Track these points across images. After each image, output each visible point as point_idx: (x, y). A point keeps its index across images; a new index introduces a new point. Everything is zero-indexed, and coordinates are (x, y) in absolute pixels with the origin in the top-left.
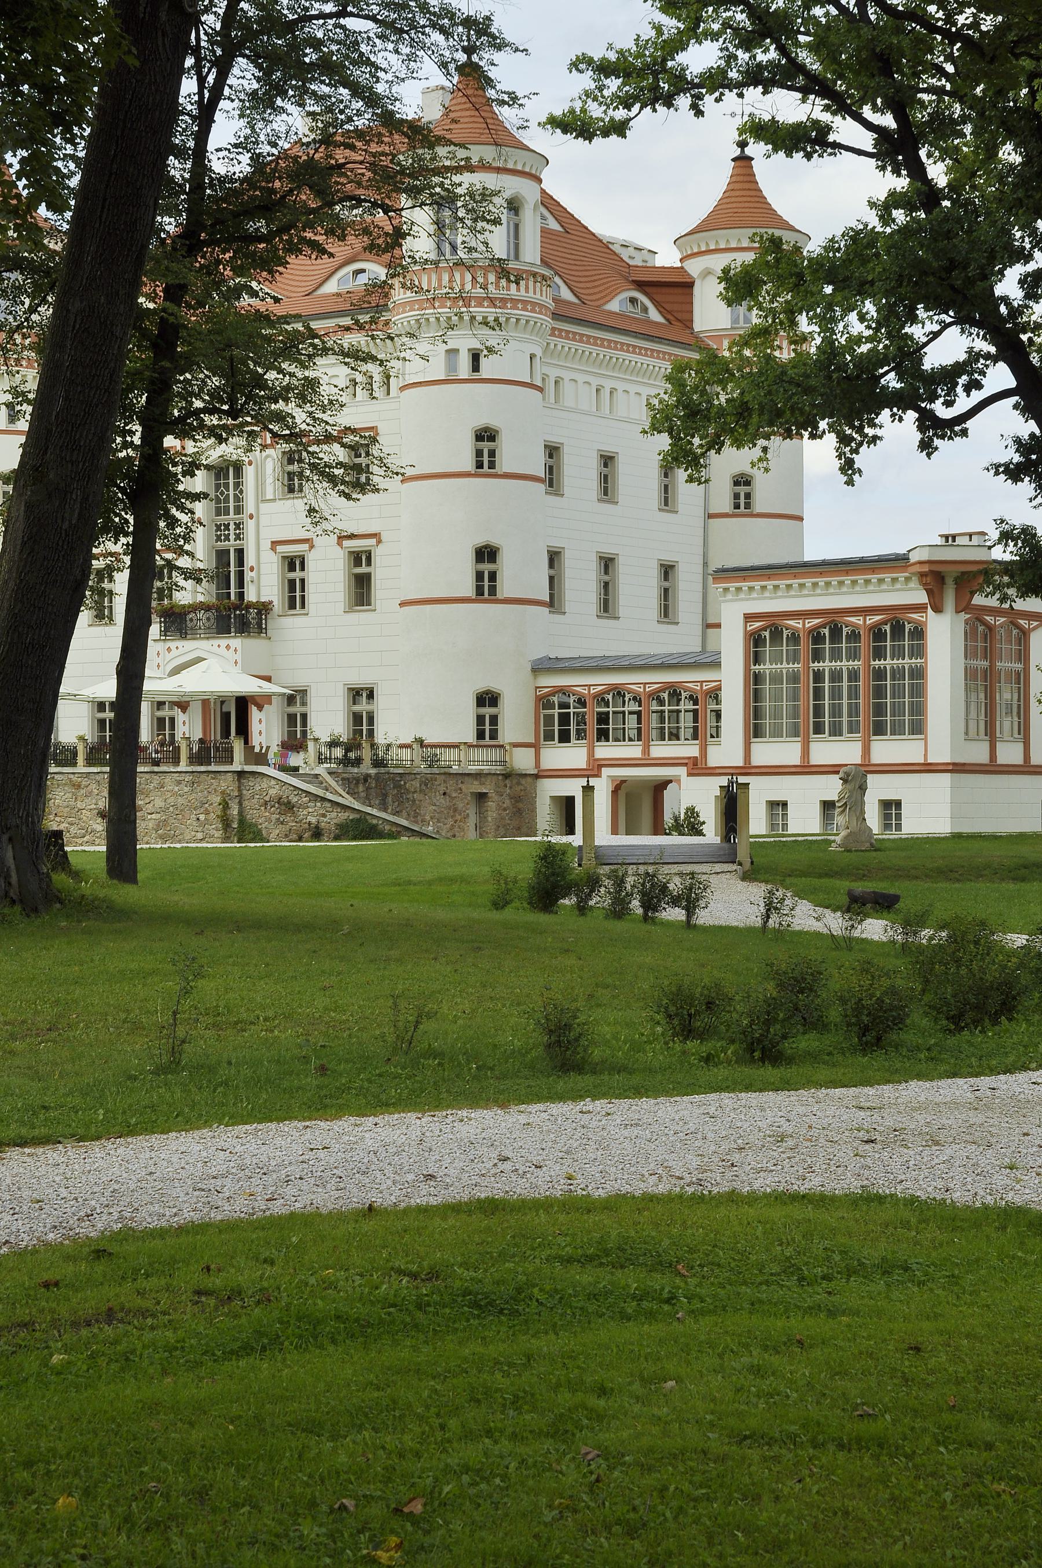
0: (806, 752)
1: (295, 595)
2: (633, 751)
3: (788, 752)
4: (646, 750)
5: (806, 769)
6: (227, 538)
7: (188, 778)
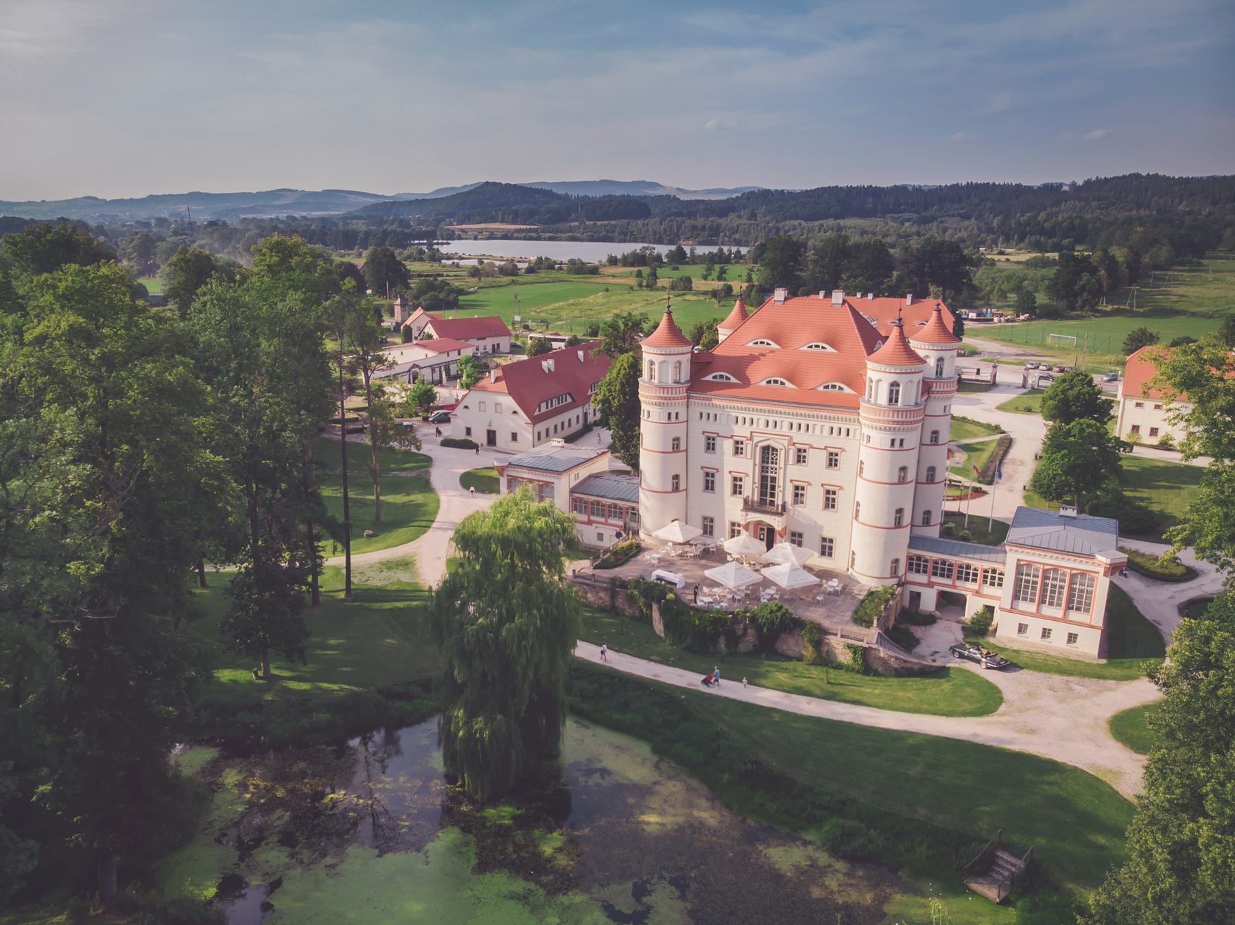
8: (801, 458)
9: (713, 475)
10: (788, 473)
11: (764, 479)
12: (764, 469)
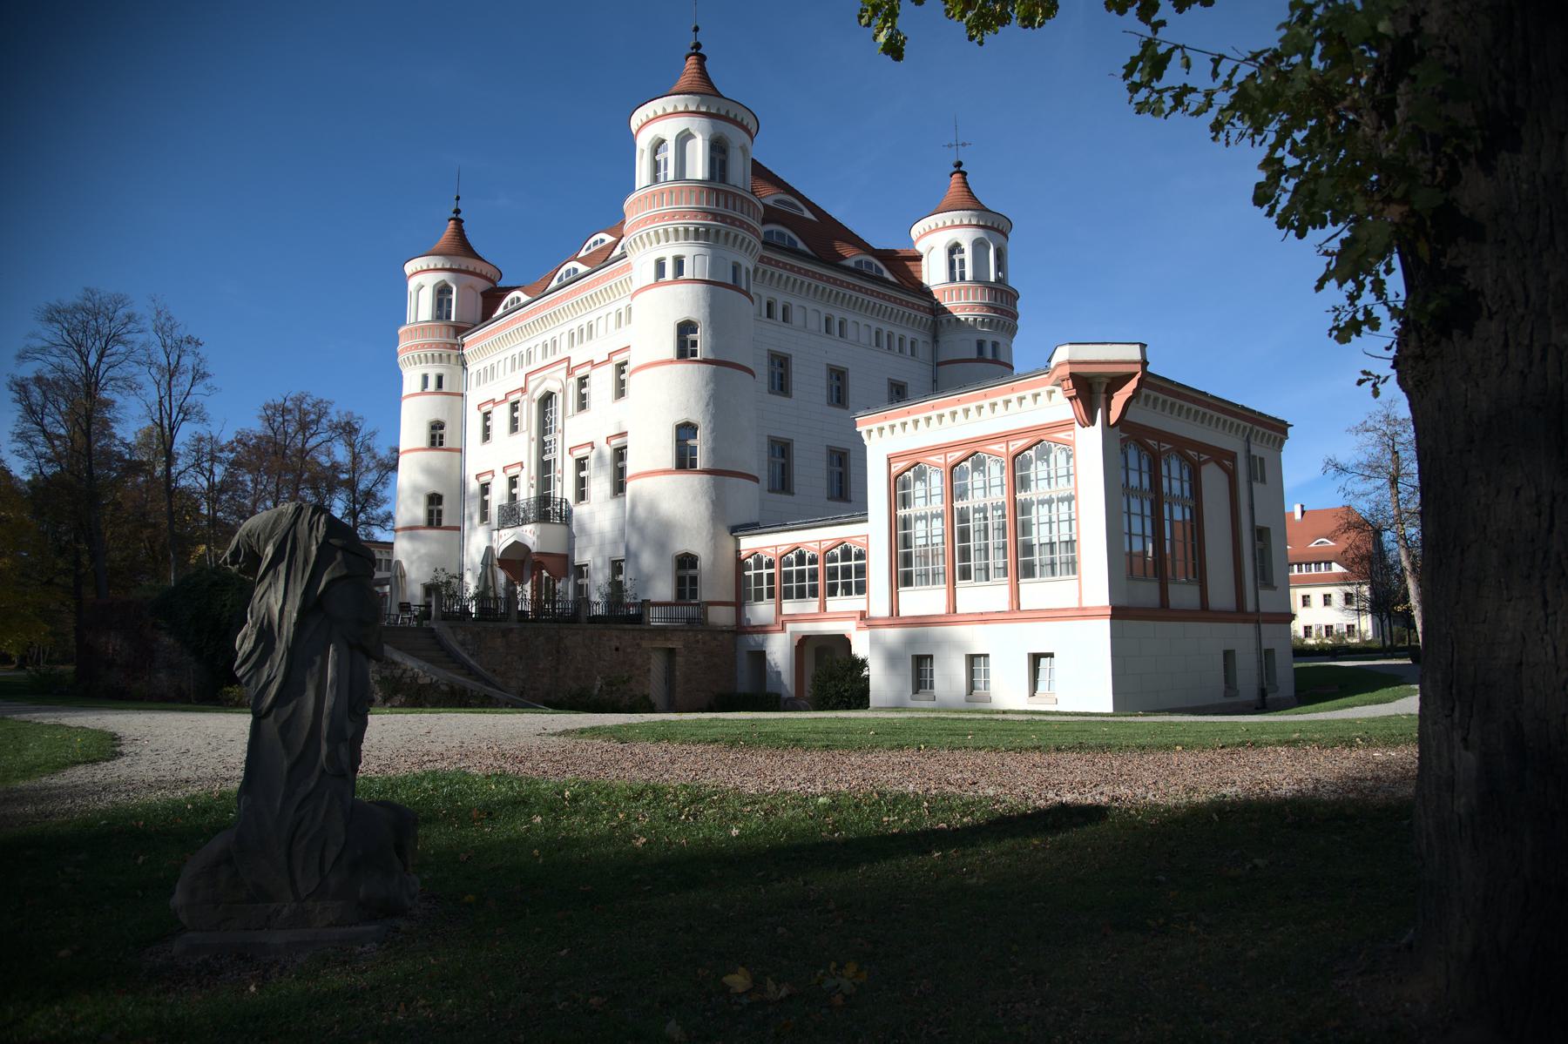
2: (812, 606)
4: (823, 607)
12: (543, 447)
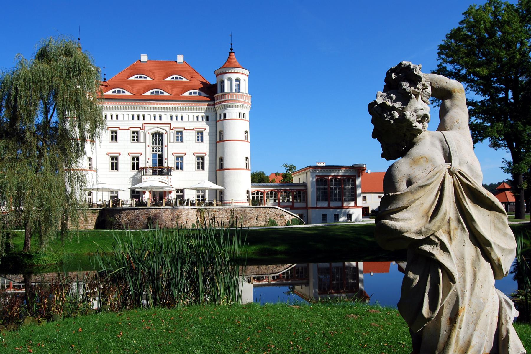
0: (329, 204)
1: (180, 167)
3: (326, 204)
5: (329, 207)
6: (156, 151)
7: (254, 209)
8: (180, 139)
9: (116, 158)
10: (171, 149)
11: (154, 156)
